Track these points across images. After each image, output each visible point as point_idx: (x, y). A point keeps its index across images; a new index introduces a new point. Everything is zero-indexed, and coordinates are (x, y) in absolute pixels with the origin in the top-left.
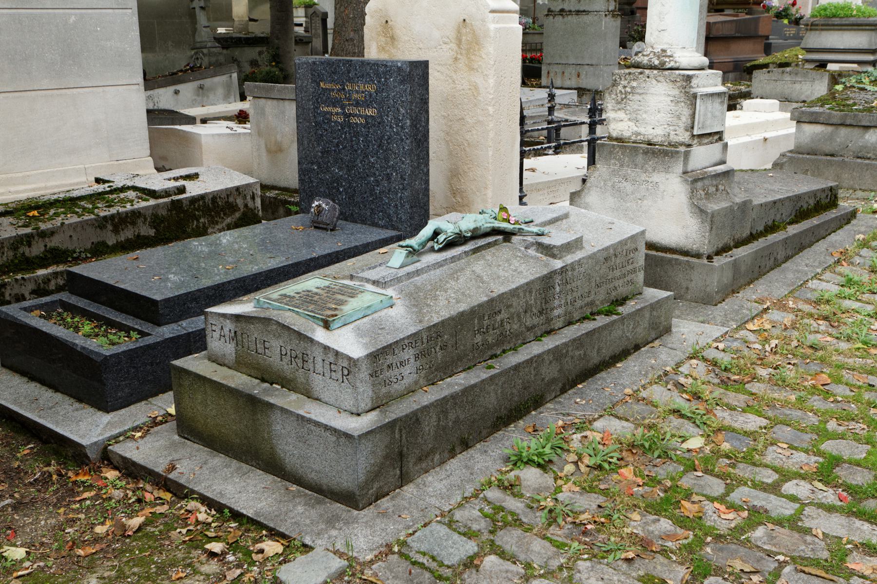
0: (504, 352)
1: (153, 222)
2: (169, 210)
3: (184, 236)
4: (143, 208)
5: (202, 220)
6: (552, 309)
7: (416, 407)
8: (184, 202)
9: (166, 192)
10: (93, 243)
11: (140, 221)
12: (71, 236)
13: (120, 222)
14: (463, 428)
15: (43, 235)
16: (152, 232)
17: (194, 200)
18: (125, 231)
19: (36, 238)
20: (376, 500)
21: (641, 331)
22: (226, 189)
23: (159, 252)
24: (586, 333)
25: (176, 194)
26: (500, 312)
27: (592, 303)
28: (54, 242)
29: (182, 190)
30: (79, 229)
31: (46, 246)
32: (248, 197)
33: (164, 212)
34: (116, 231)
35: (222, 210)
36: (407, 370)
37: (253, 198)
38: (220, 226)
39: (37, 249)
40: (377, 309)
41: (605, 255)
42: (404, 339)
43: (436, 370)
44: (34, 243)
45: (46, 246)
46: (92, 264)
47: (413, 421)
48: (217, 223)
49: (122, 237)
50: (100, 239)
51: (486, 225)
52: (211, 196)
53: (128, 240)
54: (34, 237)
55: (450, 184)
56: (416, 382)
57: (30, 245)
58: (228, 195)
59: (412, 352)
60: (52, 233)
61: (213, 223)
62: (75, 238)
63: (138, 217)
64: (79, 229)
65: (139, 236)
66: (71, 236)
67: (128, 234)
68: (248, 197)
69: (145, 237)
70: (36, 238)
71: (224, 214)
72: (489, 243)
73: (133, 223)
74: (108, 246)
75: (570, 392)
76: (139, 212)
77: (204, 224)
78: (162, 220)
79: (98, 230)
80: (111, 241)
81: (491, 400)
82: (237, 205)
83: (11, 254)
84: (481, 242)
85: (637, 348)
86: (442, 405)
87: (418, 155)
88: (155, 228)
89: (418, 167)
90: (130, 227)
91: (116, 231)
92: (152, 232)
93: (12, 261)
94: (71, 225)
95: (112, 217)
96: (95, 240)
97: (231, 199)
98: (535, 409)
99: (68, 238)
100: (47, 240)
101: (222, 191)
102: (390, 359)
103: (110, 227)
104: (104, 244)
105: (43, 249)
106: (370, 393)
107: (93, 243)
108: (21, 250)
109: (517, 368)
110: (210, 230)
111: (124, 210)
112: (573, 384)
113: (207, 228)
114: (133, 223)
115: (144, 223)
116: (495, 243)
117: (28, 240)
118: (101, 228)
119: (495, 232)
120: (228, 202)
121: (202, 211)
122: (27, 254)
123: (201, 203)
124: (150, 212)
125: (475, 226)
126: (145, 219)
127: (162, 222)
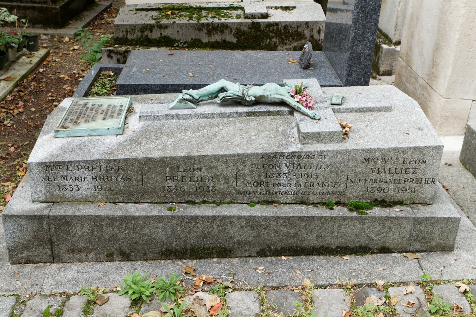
0: (204, 202)
1: (237, 34)
2: (249, 28)
3: (258, 48)
4: (230, 23)
5: (274, 40)
6: (278, 185)
7: (69, 213)
8: (262, 24)
9: (252, 15)
10: (192, 39)
11: (227, 31)
12: (178, 31)
13: (212, 29)
14: (120, 244)
15: (160, 27)
16: (235, 40)
17: (269, 25)
18: (216, 35)
19: (156, 28)
20: (27, 263)
21: (392, 238)
22: (297, 22)
23: (239, 55)
24: (300, 217)
25: (259, 18)
26: (200, 169)
27: (340, 194)
28: (167, 33)
29: (265, 16)
30: (184, 28)
31: (161, 34)
32: (315, 31)
33: (246, 29)
34: (209, 34)
35: (291, 36)
36: (83, 185)
37: (319, 32)
38: (288, 47)
39: (155, 35)
40: (103, 133)
41: (366, 155)
42: (79, 161)
43: (117, 193)
44: (154, 30)
45: (161, 34)
46: (185, 51)
47: (63, 223)
48: (286, 44)
49: (213, 39)
50: (197, 37)
51: (273, 96)
52: (283, 25)
53: (216, 42)
54: (154, 27)
55: (433, 56)
56: (94, 197)
57: (151, 32)
58: (298, 26)
59: (88, 173)
60: (166, 27)
61: (282, 43)
62: (180, 33)
63: (226, 28)
64: (184, 28)
65: (225, 41)
66: (178, 31)
67: (217, 38)
68: (315, 31)
69: (230, 43)
70: (156, 28)
71: (293, 39)
72: (269, 112)
73: (222, 32)
74: (202, 43)
75: (269, 259)
76: (227, 26)
77: (275, 43)
78: (244, 33)
79: (197, 31)
80: (205, 40)
81: (160, 234)
82: (304, 35)
83: (139, 34)
84: (241, 109)
85: (385, 250)
86: (97, 221)
87: (365, 25)
88: (237, 38)
89: (362, 35)
90: (219, 33)
91: (209, 34)
92: (235, 40)
93: (140, 38)
94: (179, 24)
95: (208, 25)
96: (194, 38)
97: (300, 30)
98: (218, 257)
99: (176, 32)
100: (162, 30)
101: (293, 22)
102: (63, 172)
103: (205, 31)
104: (199, 40)
105: (159, 35)
106: (44, 190)
107: (192, 39)
108: (146, 33)
109: (194, 219)
110: (279, 48)
111: (219, 21)
112: (278, 253)
113: (277, 46)
114: (222, 32)
115: (230, 33)
116: (278, 113)
117: (151, 28)
118: (199, 30)
119: (283, 103)
120: (297, 31)
121: (276, 34)
122: (149, 36)
123: (275, 28)
124: (236, 26)
125: (262, 94)
126: (231, 31)
127: (243, 35)
